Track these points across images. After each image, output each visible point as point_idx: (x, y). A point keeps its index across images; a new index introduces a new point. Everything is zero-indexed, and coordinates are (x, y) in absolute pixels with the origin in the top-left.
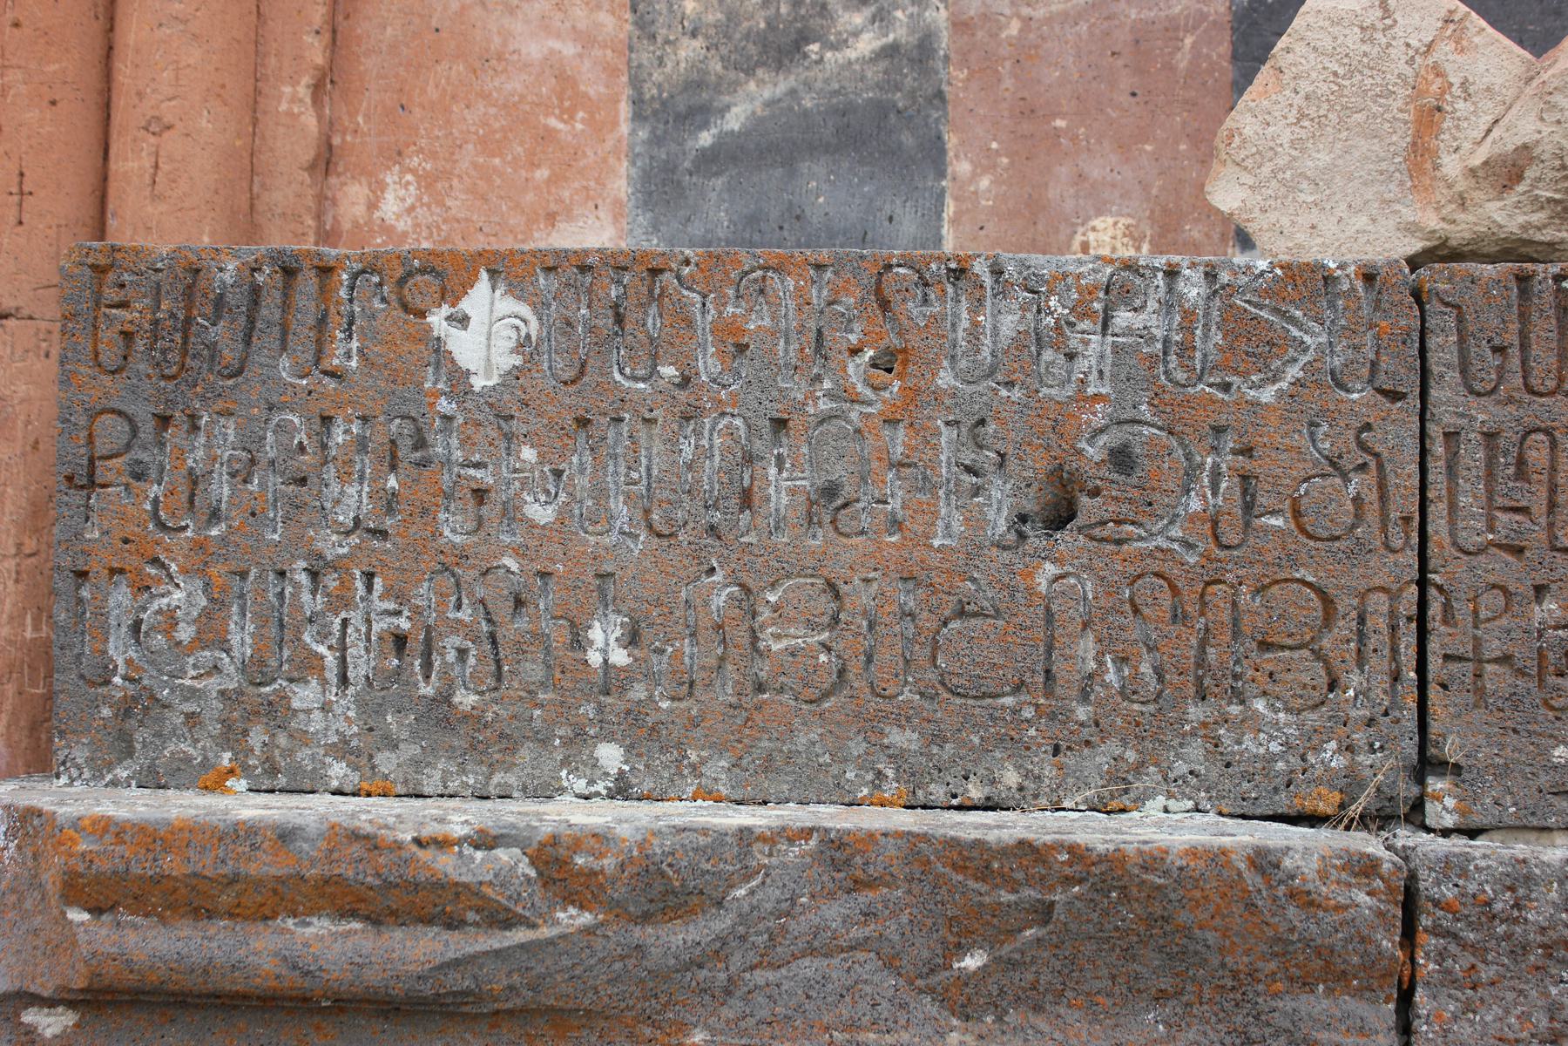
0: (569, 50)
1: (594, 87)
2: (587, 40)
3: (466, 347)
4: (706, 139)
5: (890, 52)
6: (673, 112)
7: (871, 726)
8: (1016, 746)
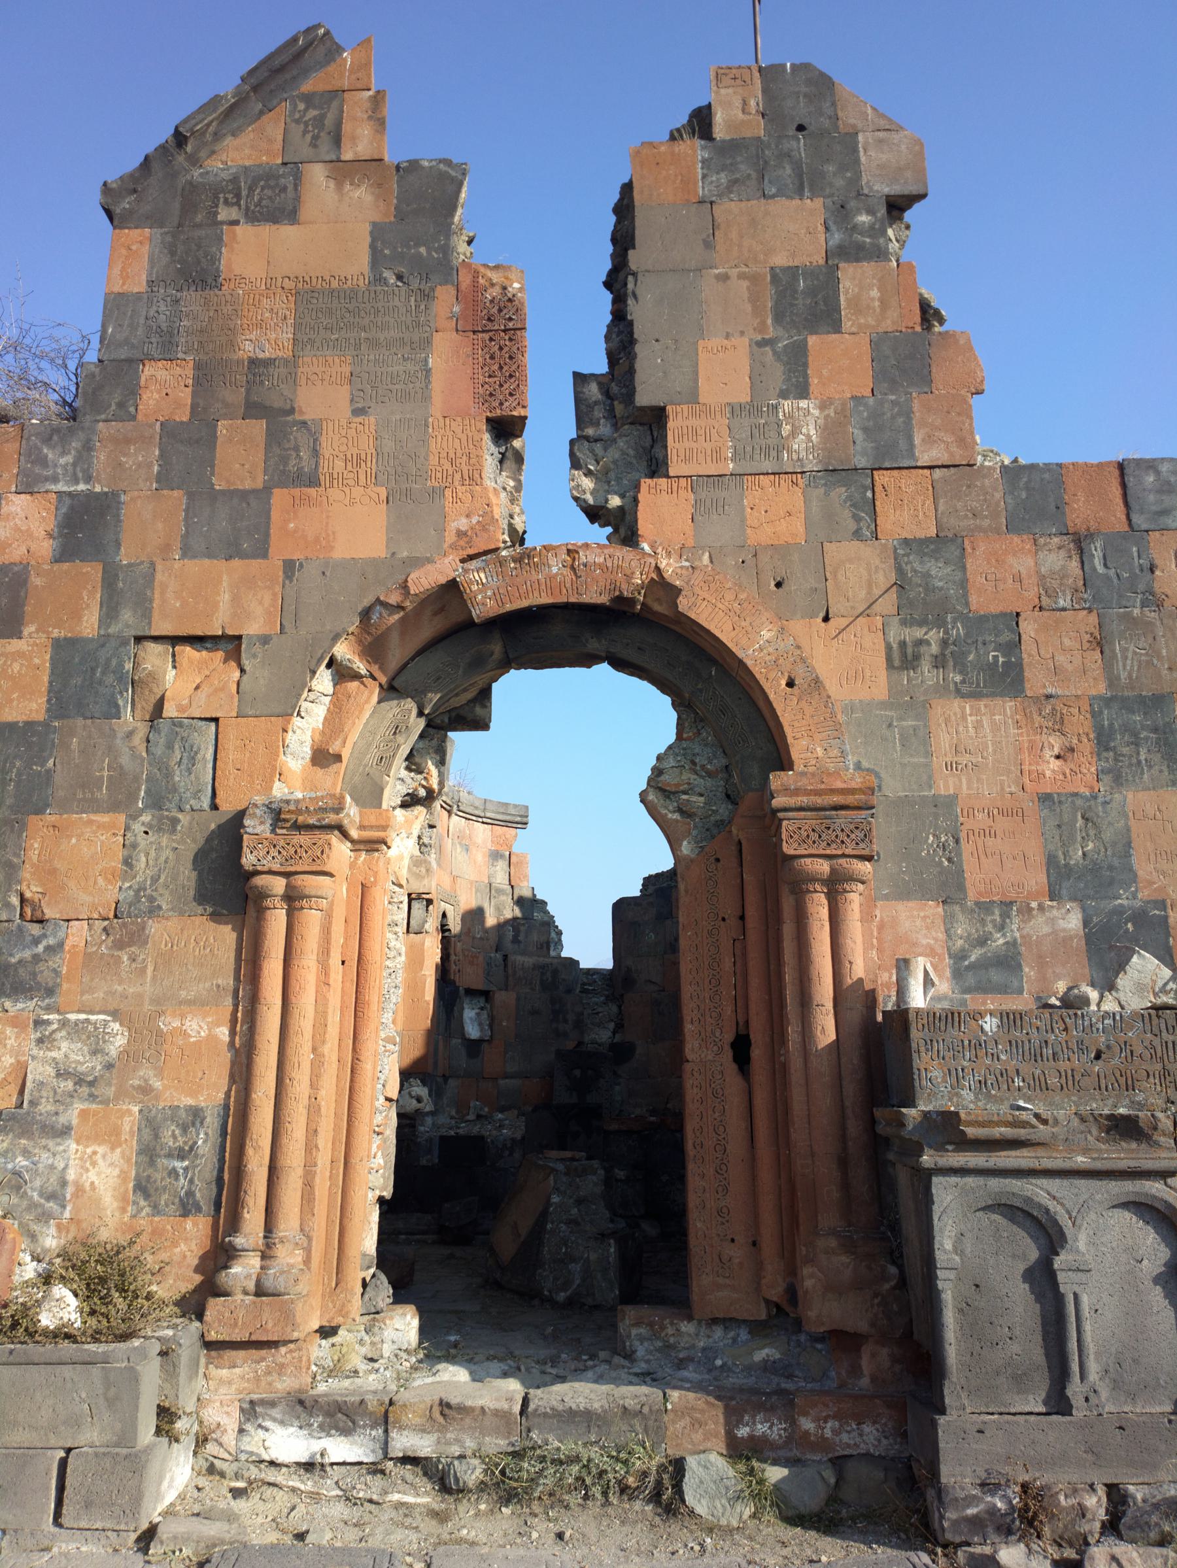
0: (932, 942)
1: (939, 951)
2: (936, 940)
3: (987, 1027)
4: (966, 963)
5: (1007, 943)
6: (958, 957)
7: (1068, 1096)
8: (1095, 1100)
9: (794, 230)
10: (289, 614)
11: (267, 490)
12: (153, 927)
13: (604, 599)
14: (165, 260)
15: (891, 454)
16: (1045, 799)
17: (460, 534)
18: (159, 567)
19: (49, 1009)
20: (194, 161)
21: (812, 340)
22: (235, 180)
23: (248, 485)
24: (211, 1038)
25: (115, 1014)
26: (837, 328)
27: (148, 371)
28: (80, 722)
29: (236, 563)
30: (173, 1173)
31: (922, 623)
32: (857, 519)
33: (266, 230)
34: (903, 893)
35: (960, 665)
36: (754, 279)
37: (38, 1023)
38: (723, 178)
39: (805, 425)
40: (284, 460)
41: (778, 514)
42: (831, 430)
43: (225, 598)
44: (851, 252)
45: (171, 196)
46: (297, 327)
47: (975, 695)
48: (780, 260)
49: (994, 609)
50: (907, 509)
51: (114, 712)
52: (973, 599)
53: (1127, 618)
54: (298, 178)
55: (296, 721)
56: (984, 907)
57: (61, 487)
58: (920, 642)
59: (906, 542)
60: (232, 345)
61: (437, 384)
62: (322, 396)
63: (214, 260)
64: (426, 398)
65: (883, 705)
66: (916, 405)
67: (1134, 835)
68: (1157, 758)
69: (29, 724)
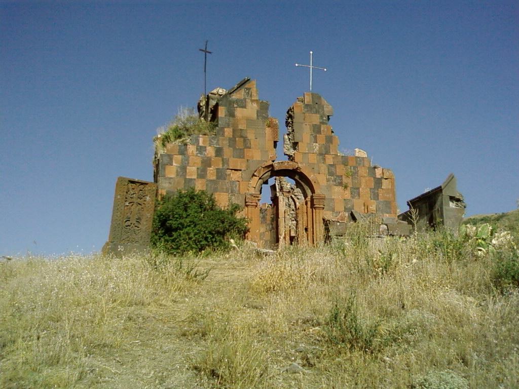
9: (316, 119)
10: (248, 167)
13: (291, 169)
14: (227, 112)
15: (327, 152)
16: (345, 200)
18: (230, 159)
20: (230, 97)
21: (318, 135)
22: (236, 100)
23: (241, 148)
26: (321, 134)
27: (226, 129)
29: (240, 159)
31: (331, 176)
33: (241, 109)
34: (328, 210)
38: (306, 110)
39: (316, 147)
40: (246, 145)
41: (313, 159)
43: (239, 164)
44: (323, 123)
46: (247, 125)
47: (337, 186)
48: (314, 123)
50: (330, 160)
53: (355, 178)
56: (337, 212)
59: (329, 165)
60: (238, 127)
61: (267, 135)
62: (251, 136)
63: (234, 113)
64: (265, 137)
69: (214, 180)
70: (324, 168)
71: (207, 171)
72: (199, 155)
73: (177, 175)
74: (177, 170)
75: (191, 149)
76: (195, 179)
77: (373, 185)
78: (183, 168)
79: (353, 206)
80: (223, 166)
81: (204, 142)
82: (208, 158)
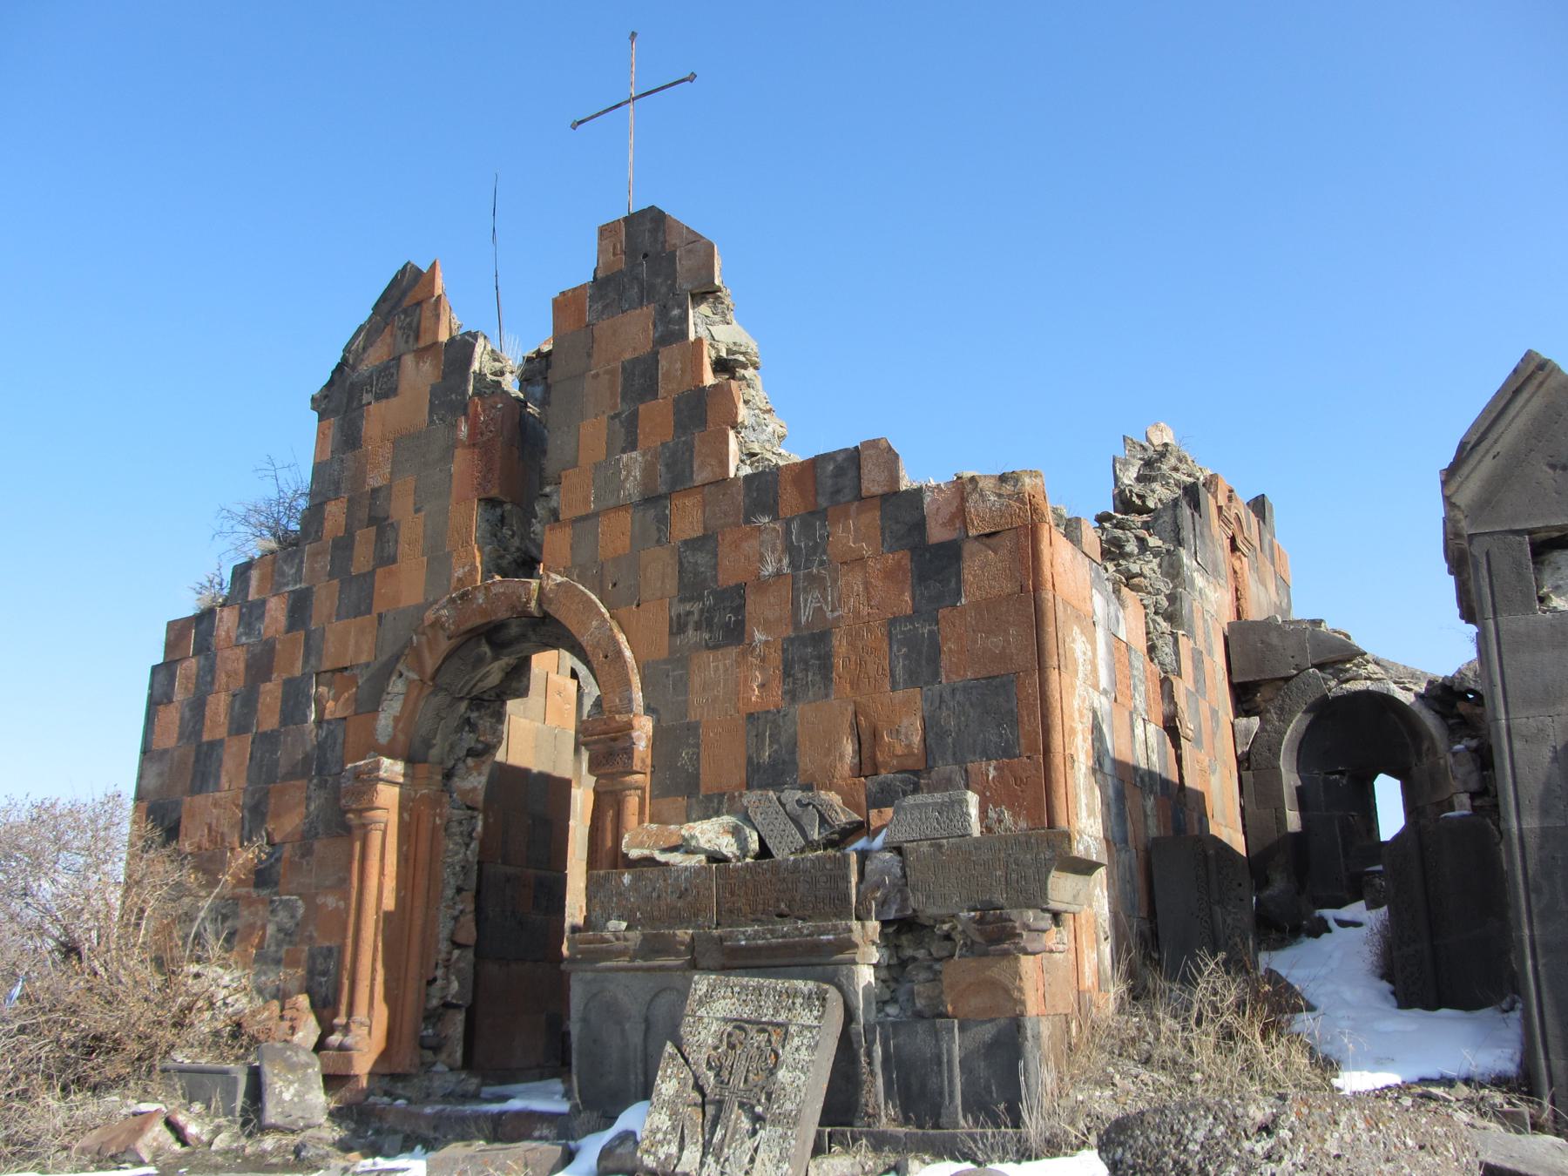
11: (372, 573)
12: (317, 845)
17: (459, 580)
19: (276, 894)
20: (353, 368)
21: (642, 407)
22: (371, 377)
24: (337, 908)
25: (300, 895)
28: (292, 727)
30: (320, 984)
31: (691, 599)
32: (659, 530)
33: (384, 402)
35: (710, 626)
36: (612, 372)
37: (272, 902)
38: (599, 306)
41: (616, 534)
42: (648, 470)
45: (342, 400)
47: (716, 647)
48: (628, 356)
49: (732, 583)
50: (688, 519)
51: (305, 719)
52: (720, 577)
54: (398, 366)
55: (382, 715)
56: (709, 798)
57: (290, 588)
58: (689, 613)
59: (685, 542)
65: (666, 661)
66: (696, 443)
67: (800, 738)
68: (818, 678)
70: (660, 572)
71: (257, 701)
72: (244, 639)
73: (181, 736)
74: (182, 719)
75: (227, 621)
76: (221, 742)
77: (907, 597)
78: (198, 706)
79: (793, 746)
80: (304, 667)
81: (262, 579)
82: (266, 642)
